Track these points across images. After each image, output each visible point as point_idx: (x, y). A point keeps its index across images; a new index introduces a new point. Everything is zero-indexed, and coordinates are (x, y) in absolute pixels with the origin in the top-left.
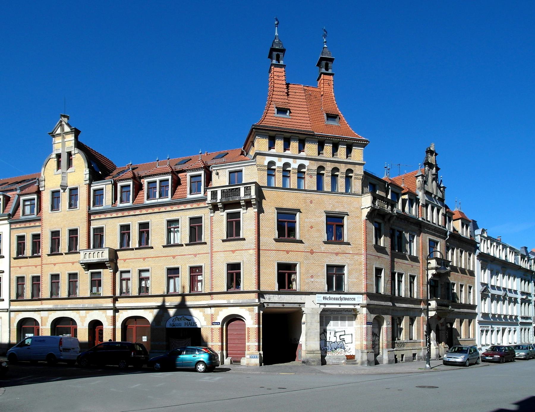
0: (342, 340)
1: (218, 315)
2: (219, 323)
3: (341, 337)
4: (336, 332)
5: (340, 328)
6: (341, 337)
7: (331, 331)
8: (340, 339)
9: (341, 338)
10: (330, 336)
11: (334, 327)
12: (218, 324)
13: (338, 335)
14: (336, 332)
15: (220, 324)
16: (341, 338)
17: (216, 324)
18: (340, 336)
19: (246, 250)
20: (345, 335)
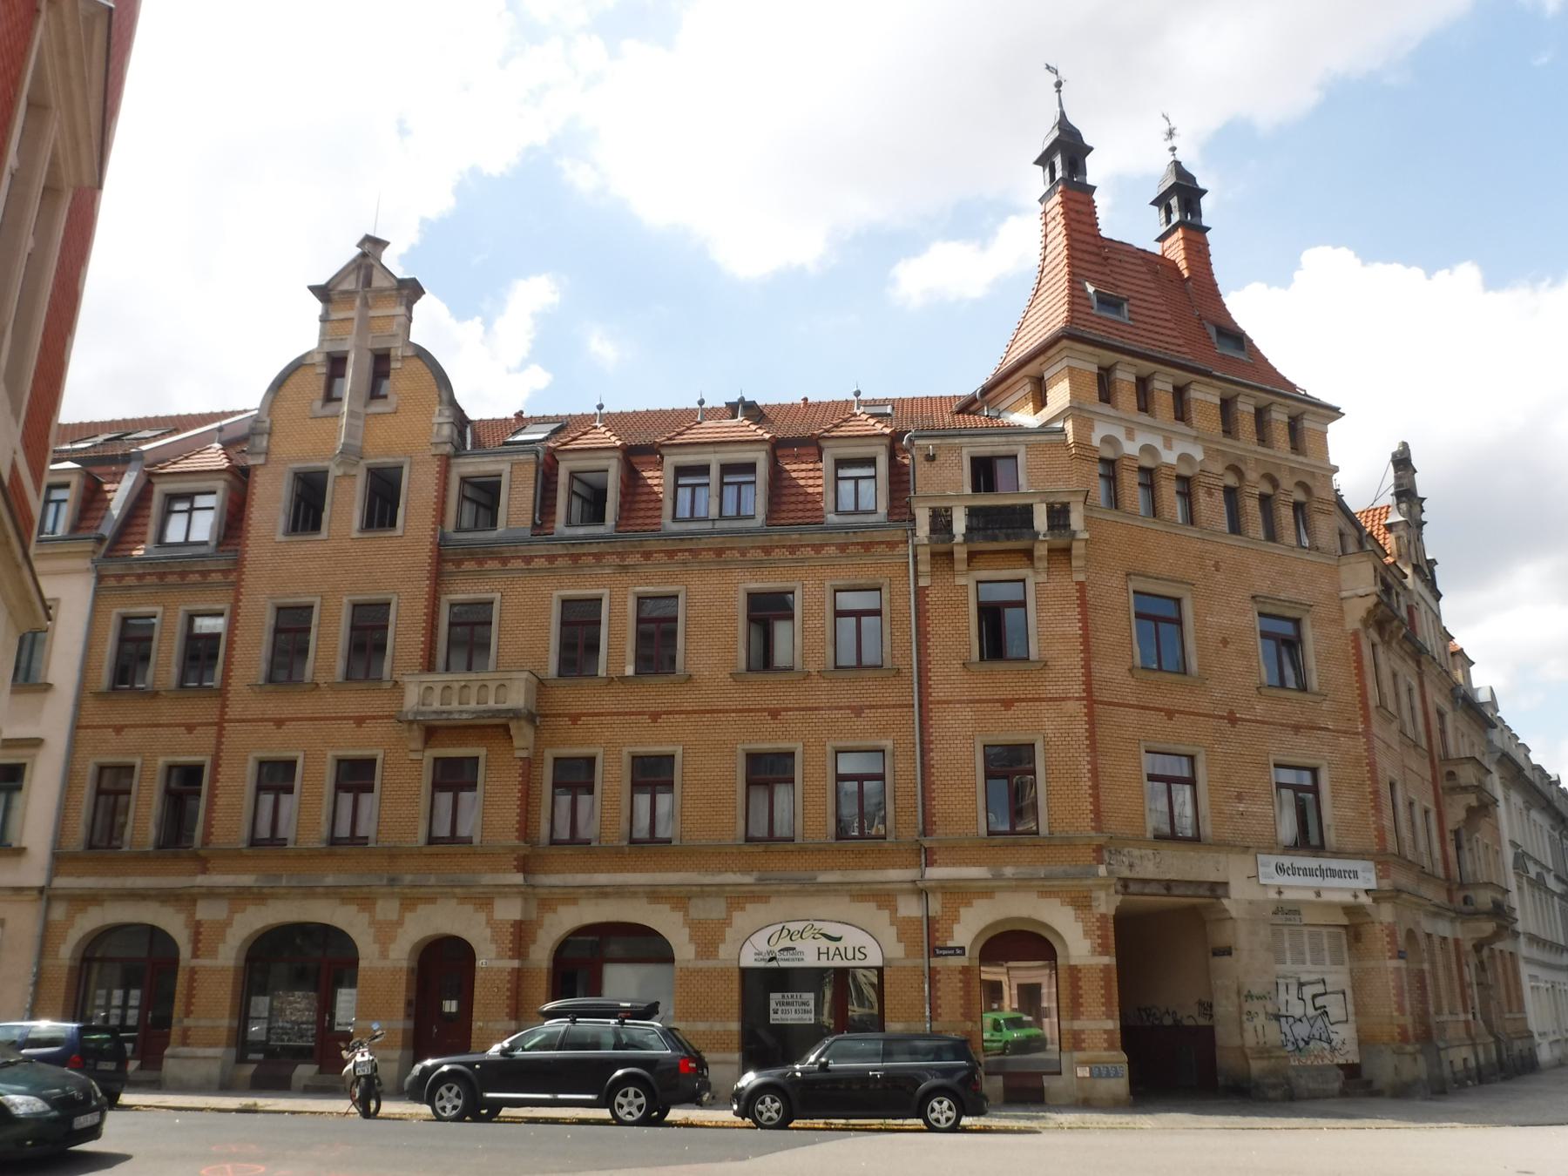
0: (1319, 1011)
1: (956, 919)
2: (963, 948)
3: (1319, 1002)
4: (1301, 985)
5: (1310, 972)
6: (1319, 1002)
7: (1288, 981)
8: (1316, 1009)
9: (1317, 1006)
10: (1288, 998)
11: (1295, 967)
12: (958, 952)
13: (1308, 992)
14: (1301, 985)
15: (964, 954)
16: (1317, 1006)
17: (950, 952)
18: (1314, 997)
19: (1051, 699)
20: (1325, 994)
